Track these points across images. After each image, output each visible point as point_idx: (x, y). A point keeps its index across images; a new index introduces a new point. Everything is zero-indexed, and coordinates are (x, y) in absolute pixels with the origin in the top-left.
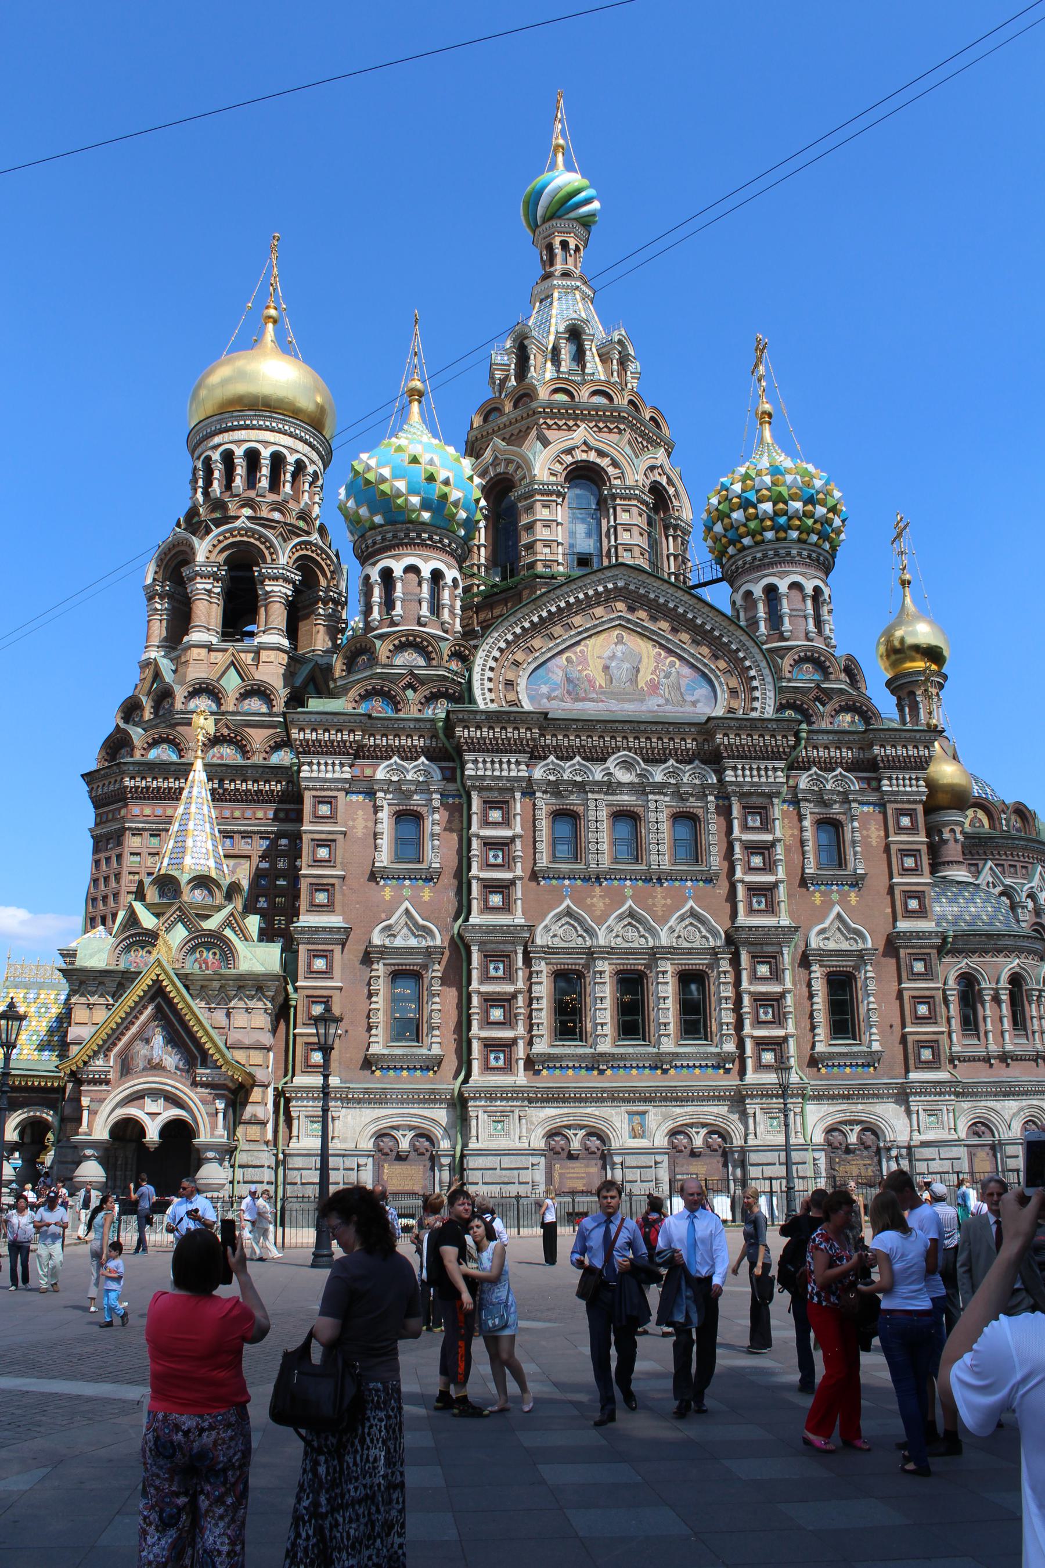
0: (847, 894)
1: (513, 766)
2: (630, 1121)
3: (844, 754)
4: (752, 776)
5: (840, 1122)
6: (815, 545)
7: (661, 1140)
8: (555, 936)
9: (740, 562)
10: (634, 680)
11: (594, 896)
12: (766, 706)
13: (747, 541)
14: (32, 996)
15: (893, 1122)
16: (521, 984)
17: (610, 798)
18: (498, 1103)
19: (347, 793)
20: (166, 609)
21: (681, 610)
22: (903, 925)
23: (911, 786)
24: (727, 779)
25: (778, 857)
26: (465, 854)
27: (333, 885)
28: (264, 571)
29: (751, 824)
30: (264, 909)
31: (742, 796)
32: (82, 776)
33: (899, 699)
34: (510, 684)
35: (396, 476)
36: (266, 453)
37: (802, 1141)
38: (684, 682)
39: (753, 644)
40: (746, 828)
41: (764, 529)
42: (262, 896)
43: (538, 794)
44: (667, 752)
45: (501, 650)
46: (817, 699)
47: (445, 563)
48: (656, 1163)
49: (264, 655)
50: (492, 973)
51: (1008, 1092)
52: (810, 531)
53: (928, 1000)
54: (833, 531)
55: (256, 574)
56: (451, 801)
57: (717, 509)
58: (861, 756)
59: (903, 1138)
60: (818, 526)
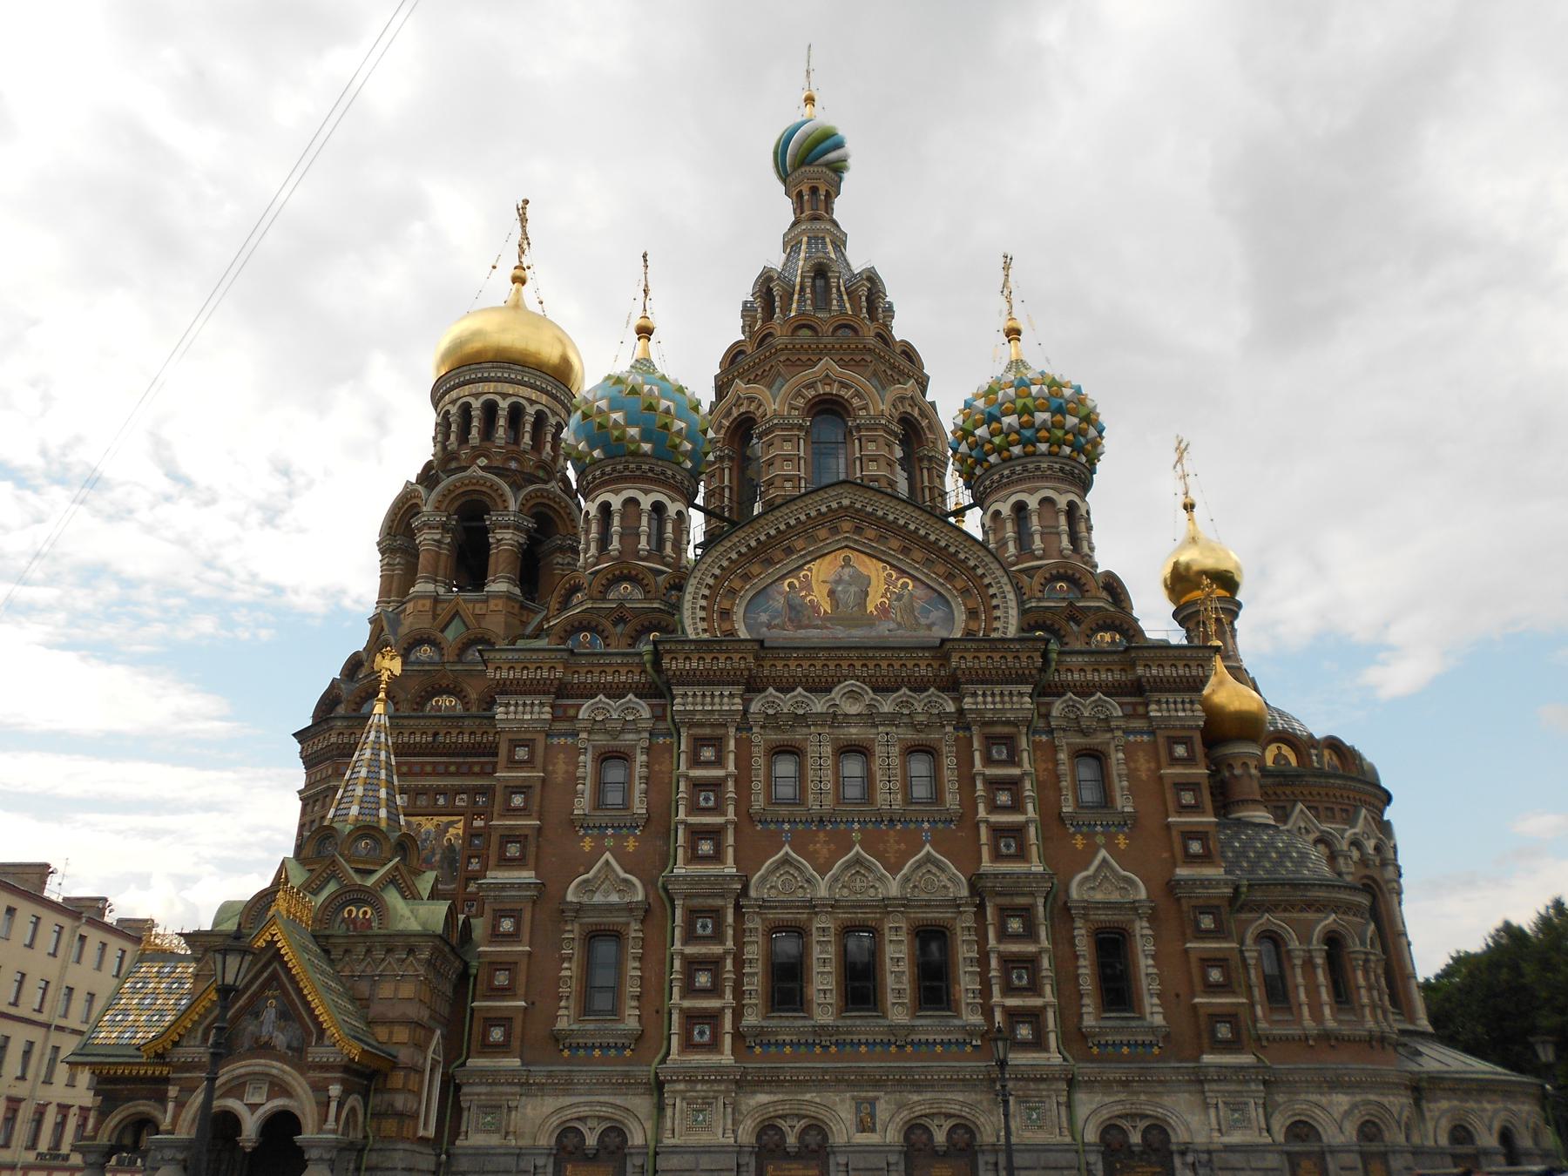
0: (1115, 836)
1: (726, 700)
2: (858, 1110)
3: (1103, 676)
4: (994, 703)
5: (1119, 1117)
6: (1069, 457)
7: (893, 1136)
8: (772, 887)
9: (988, 482)
11: (818, 842)
12: (1010, 624)
13: (993, 459)
14: (167, 970)
15: (1188, 1118)
16: (730, 944)
17: (836, 731)
18: (699, 1087)
19: (548, 735)
20: (398, 564)
21: (912, 527)
22: (1182, 872)
23: (1184, 710)
24: (966, 707)
25: (1027, 793)
27: (526, 836)
28: (494, 518)
29: (995, 756)
30: (477, 871)
31: (985, 724)
32: (294, 735)
33: (1188, 631)
34: (726, 614)
35: (613, 409)
36: (504, 404)
37: (1068, 1139)
38: (918, 604)
39: (992, 559)
40: (988, 761)
41: (1011, 444)
42: (475, 857)
43: (755, 730)
44: (899, 680)
46: (1072, 618)
47: (669, 496)
48: (888, 1164)
49: (492, 604)
50: (700, 931)
51: (1335, 1085)
52: (1061, 443)
53: (1219, 961)
54: (1088, 442)
55: (488, 523)
56: (661, 740)
57: (962, 429)
58: (1124, 678)
59: (1201, 1139)
60: (1070, 437)
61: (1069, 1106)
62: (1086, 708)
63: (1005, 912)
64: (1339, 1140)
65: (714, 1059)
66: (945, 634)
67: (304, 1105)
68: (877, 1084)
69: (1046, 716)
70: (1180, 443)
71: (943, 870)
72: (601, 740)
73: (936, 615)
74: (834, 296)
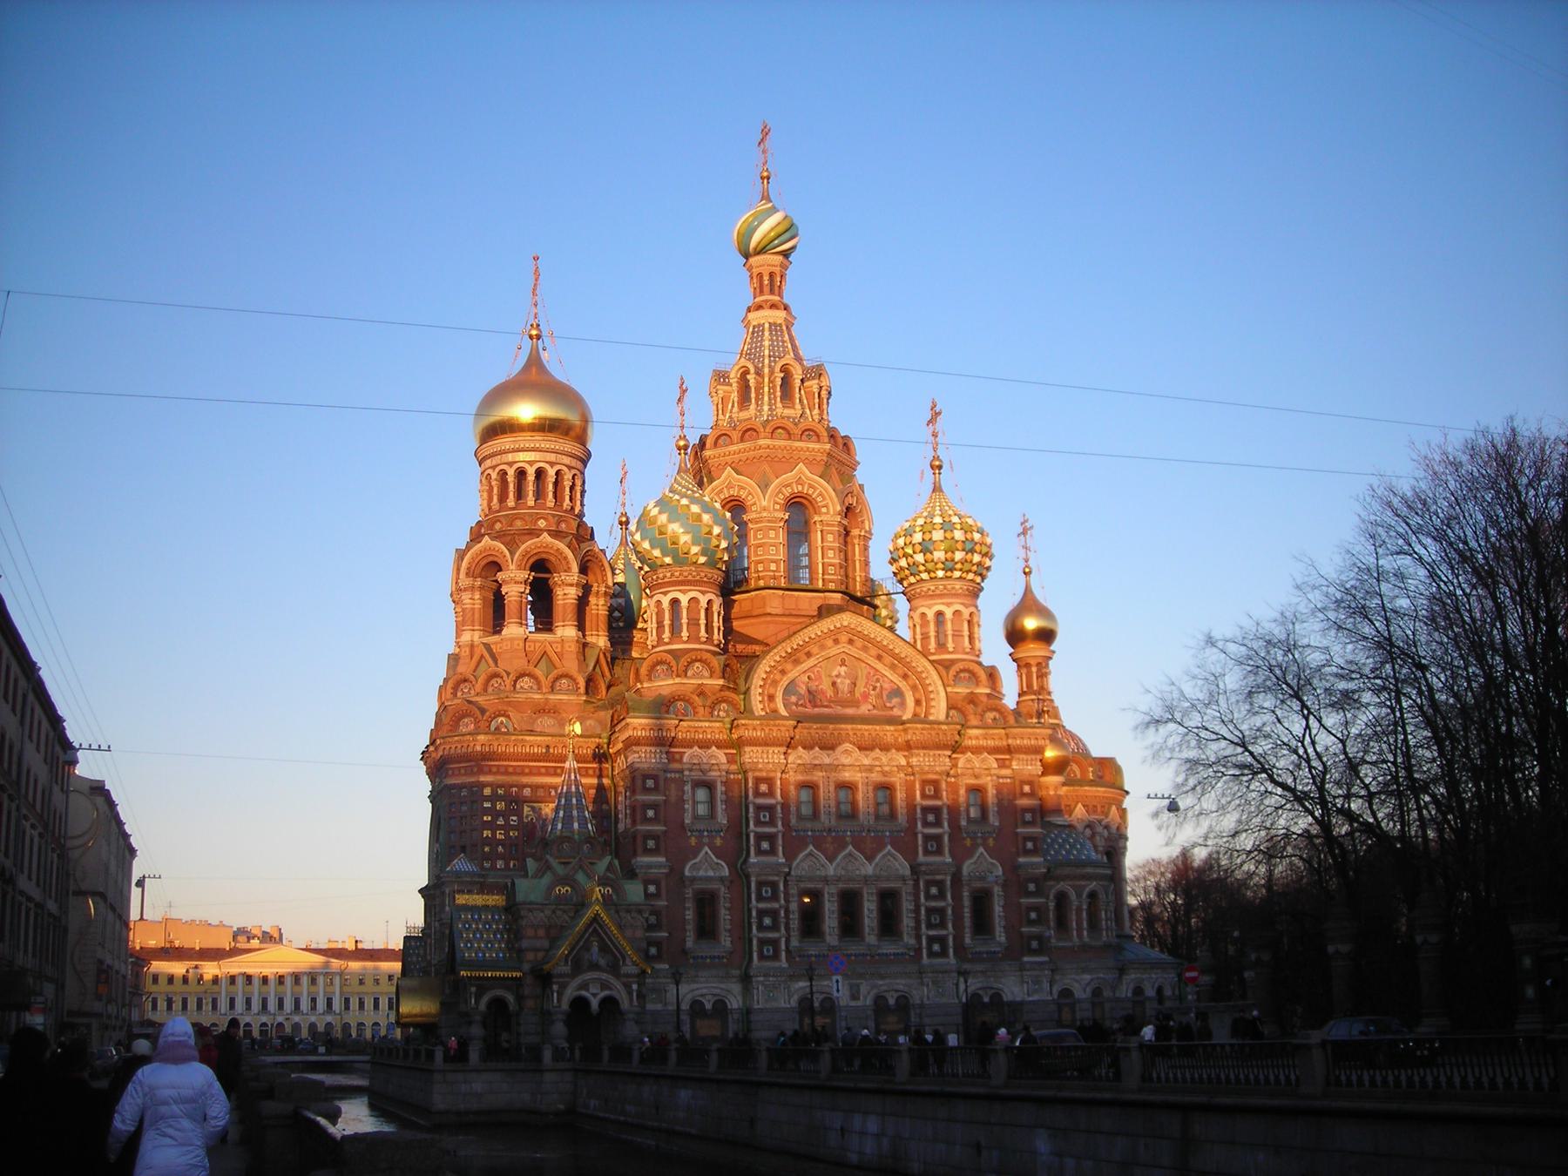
5: (980, 989)
7: (869, 1002)
10: (852, 692)
12: (939, 710)
16: (783, 902)
19: (665, 771)
22: (1021, 860)
26: (744, 814)
27: (658, 837)
34: (771, 698)
36: (551, 472)
43: (791, 773)
45: (766, 672)
51: (1085, 970)
53: (1036, 908)
56: (732, 776)
60: (975, 568)
61: (957, 985)
62: (976, 761)
63: (929, 884)
64: (1084, 996)
65: (777, 964)
66: (899, 713)
67: (619, 992)
68: (861, 976)
69: (955, 766)
70: (1026, 521)
71: (897, 860)
72: (696, 775)
73: (895, 701)
74: (797, 396)
